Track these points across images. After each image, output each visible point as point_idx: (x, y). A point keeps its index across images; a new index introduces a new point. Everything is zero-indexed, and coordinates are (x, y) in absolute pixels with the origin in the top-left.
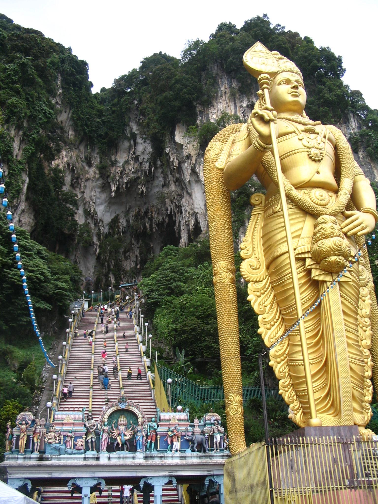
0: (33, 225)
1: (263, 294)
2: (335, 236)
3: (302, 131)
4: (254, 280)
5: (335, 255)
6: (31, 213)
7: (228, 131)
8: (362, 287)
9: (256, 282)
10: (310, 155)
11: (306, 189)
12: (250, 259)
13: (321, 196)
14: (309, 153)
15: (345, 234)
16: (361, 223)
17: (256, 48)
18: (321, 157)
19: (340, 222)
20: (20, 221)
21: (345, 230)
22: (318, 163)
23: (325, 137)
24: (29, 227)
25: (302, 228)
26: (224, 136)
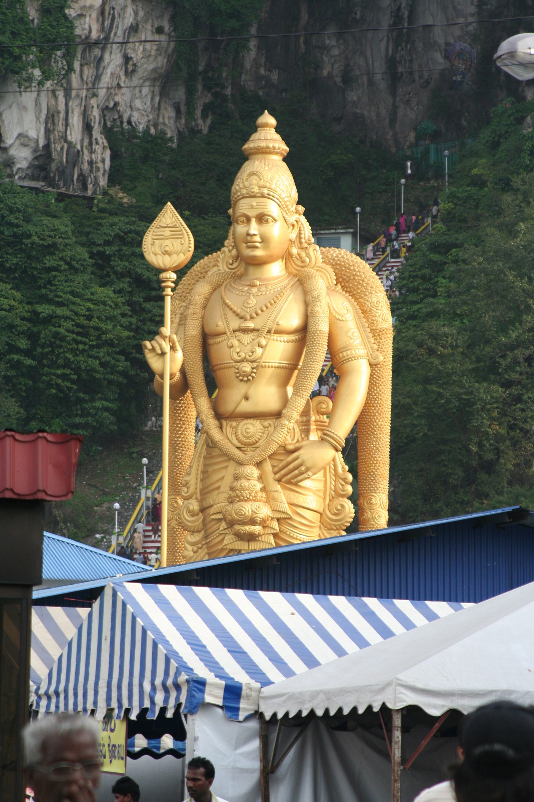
0: (170, 50)
1: (201, 548)
2: (242, 501)
3: (234, 331)
4: (192, 530)
5: (240, 524)
6: (161, 17)
7: (193, 279)
8: (337, 529)
9: (193, 532)
10: (238, 375)
11: (234, 420)
12: (190, 501)
13: (247, 433)
14: (237, 371)
15: (279, 481)
16: (301, 465)
17: (163, 220)
18: (254, 375)
19: (275, 463)
20: (127, 59)
21: (278, 476)
22: (249, 382)
23: (269, 332)
24: (160, 59)
25: (222, 478)
26: (187, 289)
